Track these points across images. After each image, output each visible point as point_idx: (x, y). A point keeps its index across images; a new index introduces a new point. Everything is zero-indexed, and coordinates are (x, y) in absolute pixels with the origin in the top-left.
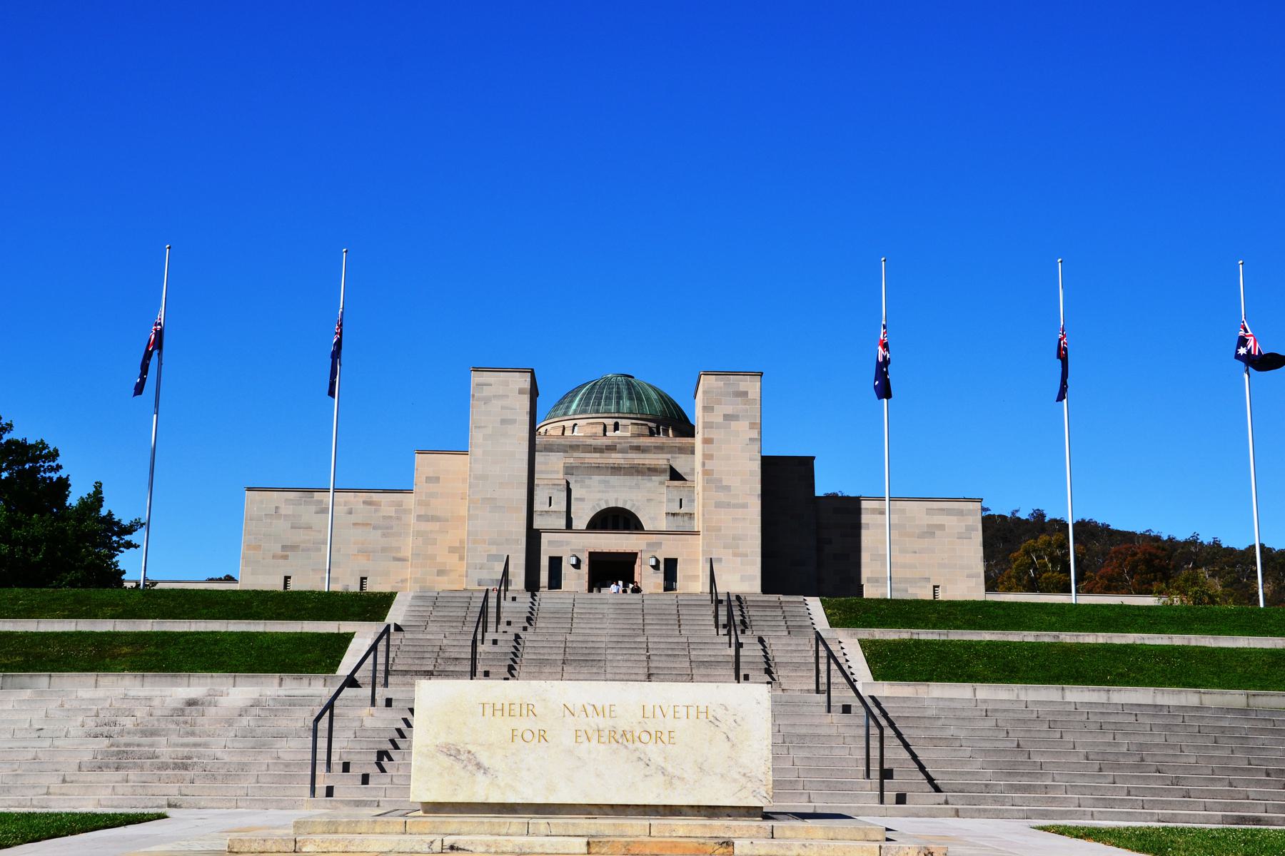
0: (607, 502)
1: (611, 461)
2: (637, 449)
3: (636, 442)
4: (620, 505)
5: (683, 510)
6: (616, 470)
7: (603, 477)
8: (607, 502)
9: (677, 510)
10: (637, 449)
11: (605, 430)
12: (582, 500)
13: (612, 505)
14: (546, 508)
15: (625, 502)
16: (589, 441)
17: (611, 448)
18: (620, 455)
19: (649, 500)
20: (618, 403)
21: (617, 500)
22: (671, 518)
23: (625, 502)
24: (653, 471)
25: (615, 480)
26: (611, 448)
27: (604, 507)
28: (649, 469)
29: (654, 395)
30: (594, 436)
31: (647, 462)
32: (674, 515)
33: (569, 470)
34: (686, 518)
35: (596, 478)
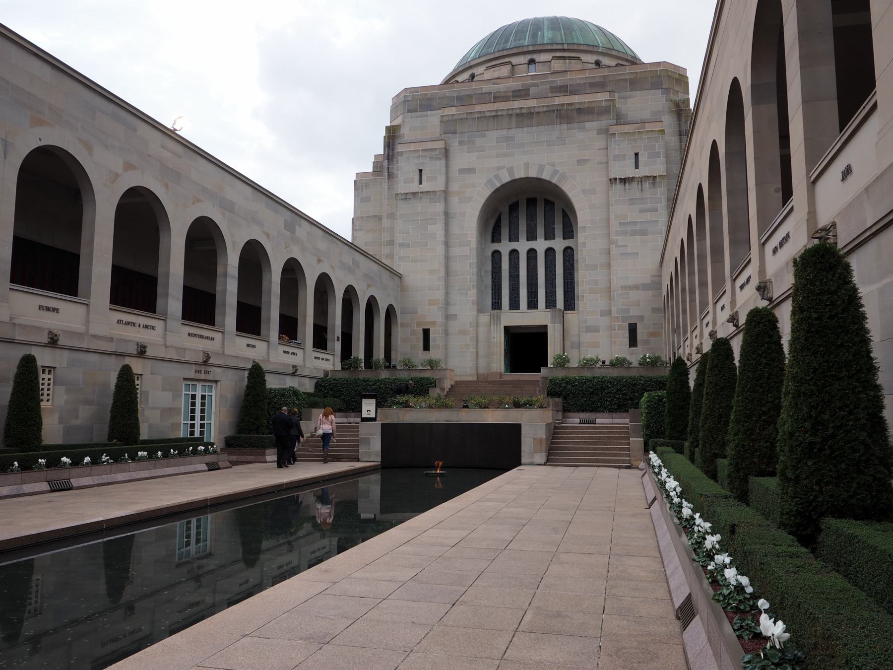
0: (510, 170)
2: (563, 89)
3: (559, 80)
4: (533, 174)
6: (525, 118)
7: (504, 132)
8: (510, 170)
9: (629, 171)
10: (563, 89)
12: (470, 171)
13: (520, 174)
14: (415, 187)
15: (541, 168)
17: (521, 93)
19: (581, 162)
20: (535, 35)
21: (527, 166)
22: (619, 187)
23: (541, 168)
24: (585, 112)
25: (522, 134)
26: (521, 93)
27: (506, 179)
28: (580, 111)
32: (624, 181)
34: (646, 185)
35: (493, 134)
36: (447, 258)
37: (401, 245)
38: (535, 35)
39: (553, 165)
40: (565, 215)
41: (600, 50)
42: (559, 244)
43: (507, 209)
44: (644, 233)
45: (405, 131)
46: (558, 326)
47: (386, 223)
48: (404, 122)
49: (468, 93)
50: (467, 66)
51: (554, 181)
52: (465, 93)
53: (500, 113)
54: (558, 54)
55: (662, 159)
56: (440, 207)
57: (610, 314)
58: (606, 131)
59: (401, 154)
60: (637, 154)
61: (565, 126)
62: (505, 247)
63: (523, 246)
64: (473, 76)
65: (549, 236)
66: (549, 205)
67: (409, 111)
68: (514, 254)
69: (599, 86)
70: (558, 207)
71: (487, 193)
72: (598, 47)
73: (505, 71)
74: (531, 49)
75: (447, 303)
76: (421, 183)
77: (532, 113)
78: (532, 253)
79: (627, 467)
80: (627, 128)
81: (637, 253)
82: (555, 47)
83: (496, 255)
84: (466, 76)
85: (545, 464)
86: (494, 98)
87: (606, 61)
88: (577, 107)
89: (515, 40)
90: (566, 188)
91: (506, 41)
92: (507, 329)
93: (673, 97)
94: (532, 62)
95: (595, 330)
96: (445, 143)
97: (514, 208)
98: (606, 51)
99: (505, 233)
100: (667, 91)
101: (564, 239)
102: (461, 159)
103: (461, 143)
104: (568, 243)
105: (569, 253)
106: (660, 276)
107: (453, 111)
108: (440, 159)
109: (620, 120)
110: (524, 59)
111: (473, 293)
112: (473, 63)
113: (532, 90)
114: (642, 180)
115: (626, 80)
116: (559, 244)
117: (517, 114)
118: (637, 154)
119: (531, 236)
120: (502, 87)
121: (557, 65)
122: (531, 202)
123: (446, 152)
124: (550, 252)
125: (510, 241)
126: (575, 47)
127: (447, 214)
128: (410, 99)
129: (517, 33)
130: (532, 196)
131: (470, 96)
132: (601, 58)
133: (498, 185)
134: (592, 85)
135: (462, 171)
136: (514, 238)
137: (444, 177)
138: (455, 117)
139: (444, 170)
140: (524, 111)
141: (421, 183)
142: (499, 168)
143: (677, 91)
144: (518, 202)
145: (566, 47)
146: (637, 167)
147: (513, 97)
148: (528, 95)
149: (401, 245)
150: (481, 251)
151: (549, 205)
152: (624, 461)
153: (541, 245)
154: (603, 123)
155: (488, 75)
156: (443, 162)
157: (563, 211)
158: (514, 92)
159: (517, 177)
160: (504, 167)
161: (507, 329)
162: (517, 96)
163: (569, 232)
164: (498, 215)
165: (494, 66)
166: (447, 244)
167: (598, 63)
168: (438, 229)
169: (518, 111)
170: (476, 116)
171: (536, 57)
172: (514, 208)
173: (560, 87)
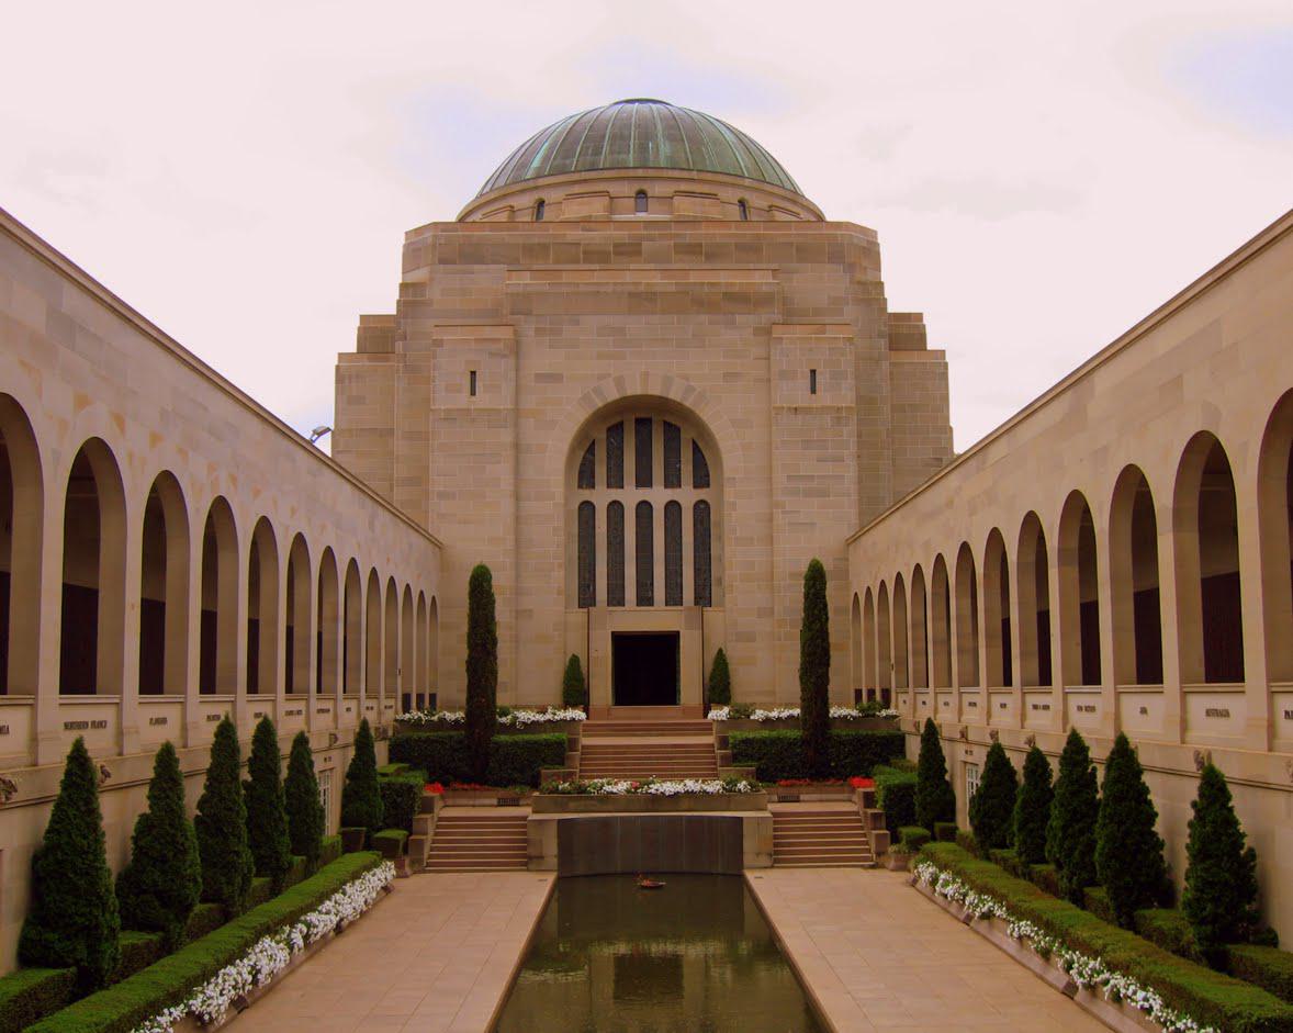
0: (619, 382)
1: (628, 277)
2: (693, 250)
4: (655, 390)
5: (824, 398)
6: (642, 300)
8: (619, 382)
9: (802, 397)
10: (693, 250)
11: (612, 211)
12: (555, 378)
13: (634, 389)
14: (463, 400)
16: (574, 234)
17: (629, 251)
18: (652, 266)
19: (730, 376)
20: (643, 149)
26: (629, 251)
27: (613, 395)
29: (729, 137)
30: (586, 222)
31: (723, 278)
33: (522, 306)
36: (517, 519)
37: (441, 495)
38: (643, 149)
39: (686, 378)
40: (696, 449)
41: (747, 182)
42: (687, 496)
43: (604, 436)
44: (823, 493)
45: (433, 293)
46: (697, 633)
47: (400, 446)
48: (432, 279)
49: (543, 241)
50: (531, 184)
51: (688, 404)
52: (536, 241)
53: (602, 289)
54: (683, 187)
55: (851, 381)
56: (506, 437)
57: (773, 613)
58: (767, 331)
59: (439, 343)
60: (813, 372)
61: (704, 318)
62: (601, 497)
63: (630, 496)
64: (541, 203)
65: (672, 481)
66: (672, 432)
67: (443, 261)
68: (616, 508)
69: (750, 250)
70: (686, 436)
71: (582, 416)
72: (743, 177)
73: (597, 208)
74: (640, 173)
75: (518, 592)
76: (473, 393)
77: (655, 293)
78: (644, 508)
79: (872, 867)
80: (799, 332)
81: (813, 524)
82: (676, 174)
83: (587, 509)
84: (527, 201)
85: (772, 867)
86: (585, 253)
87: (755, 201)
88: (724, 290)
89: (612, 152)
90: (705, 414)
91: (597, 152)
92: (613, 633)
93: (859, 276)
94: (642, 194)
95: (750, 637)
96: (515, 332)
97: (616, 431)
98: (756, 185)
99: (601, 472)
100: (851, 268)
101: (695, 487)
102: (541, 358)
103: (539, 331)
104: (702, 494)
105: (702, 509)
106: (847, 560)
107: (525, 280)
108: (504, 356)
109: (792, 314)
110: (629, 189)
111: (558, 576)
112: (541, 182)
113: (645, 245)
114: (824, 410)
115: (791, 244)
116: (687, 496)
117: (630, 294)
118: (813, 372)
119: (644, 480)
120: (596, 236)
121: (686, 207)
122: (643, 424)
123: (516, 349)
124: (673, 508)
125: (608, 487)
126: (709, 177)
127: (517, 446)
128: (442, 241)
129: (614, 137)
130: (643, 415)
131: (545, 248)
132: (747, 196)
133: (600, 405)
134: (741, 247)
135: (540, 377)
136: (616, 481)
137: (513, 384)
138: (528, 289)
139: (512, 374)
140: (642, 288)
141: (473, 393)
142: (601, 377)
143: (865, 268)
144: (622, 422)
145: (694, 175)
146: (813, 391)
147: (616, 253)
148: (639, 253)
149: (441, 495)
150: (566, 504)
151: (672, 432)
152: (865, 859)
153: (658, 496)
154: (764, 317)
155: (573, 210)
156: (512, 361)
157: (694, 442)
158: (616, 246)
159: (629, 392)
160: (610, 375)
161: (613, 633)
162: (622, 254)
163: (702, 480)
164: (588, 445)
165: (581, 195)
166: (517, 497)
167: (742, 203)
168: (503, 471)
169: (632, 288)
170: (565, 290)
171: (645, 186)
172: (616, 431)
173: (690, 245)
